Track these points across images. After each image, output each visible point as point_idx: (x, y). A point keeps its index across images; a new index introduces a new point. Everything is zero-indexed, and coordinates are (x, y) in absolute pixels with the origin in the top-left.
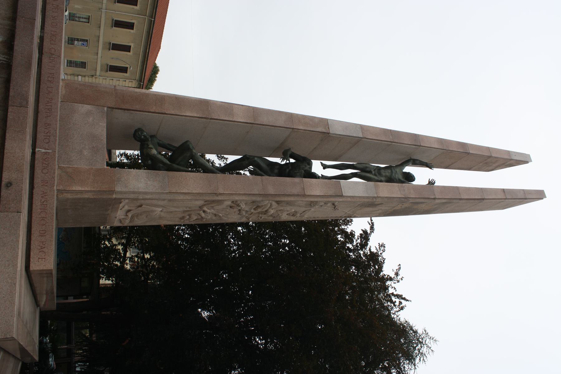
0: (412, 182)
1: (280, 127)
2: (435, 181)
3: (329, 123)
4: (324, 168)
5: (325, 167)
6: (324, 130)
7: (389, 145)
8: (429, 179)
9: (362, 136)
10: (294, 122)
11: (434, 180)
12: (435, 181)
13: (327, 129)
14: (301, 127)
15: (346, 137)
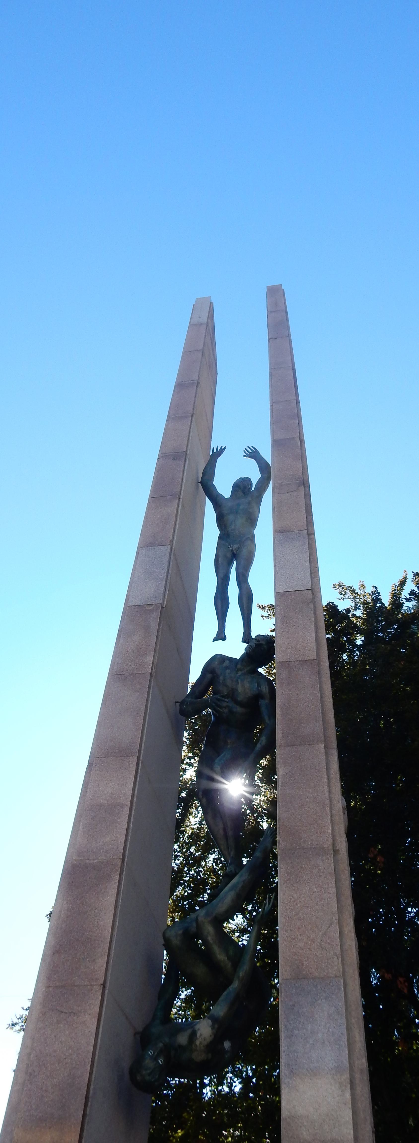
0: (252, 484)
1: (147, 701)
2: (248, 447)
3: (138, 603)
4: (224, 639)
5: (221, 636)
6: (156, 615)
7: (183, 506)
8: (244, 456)
9: (169, 547)
10: (135, 672)
11: (246, 449)
12: (248, 447)
13: (151, 608)
14: (149, 660)
15: (169, 577)
